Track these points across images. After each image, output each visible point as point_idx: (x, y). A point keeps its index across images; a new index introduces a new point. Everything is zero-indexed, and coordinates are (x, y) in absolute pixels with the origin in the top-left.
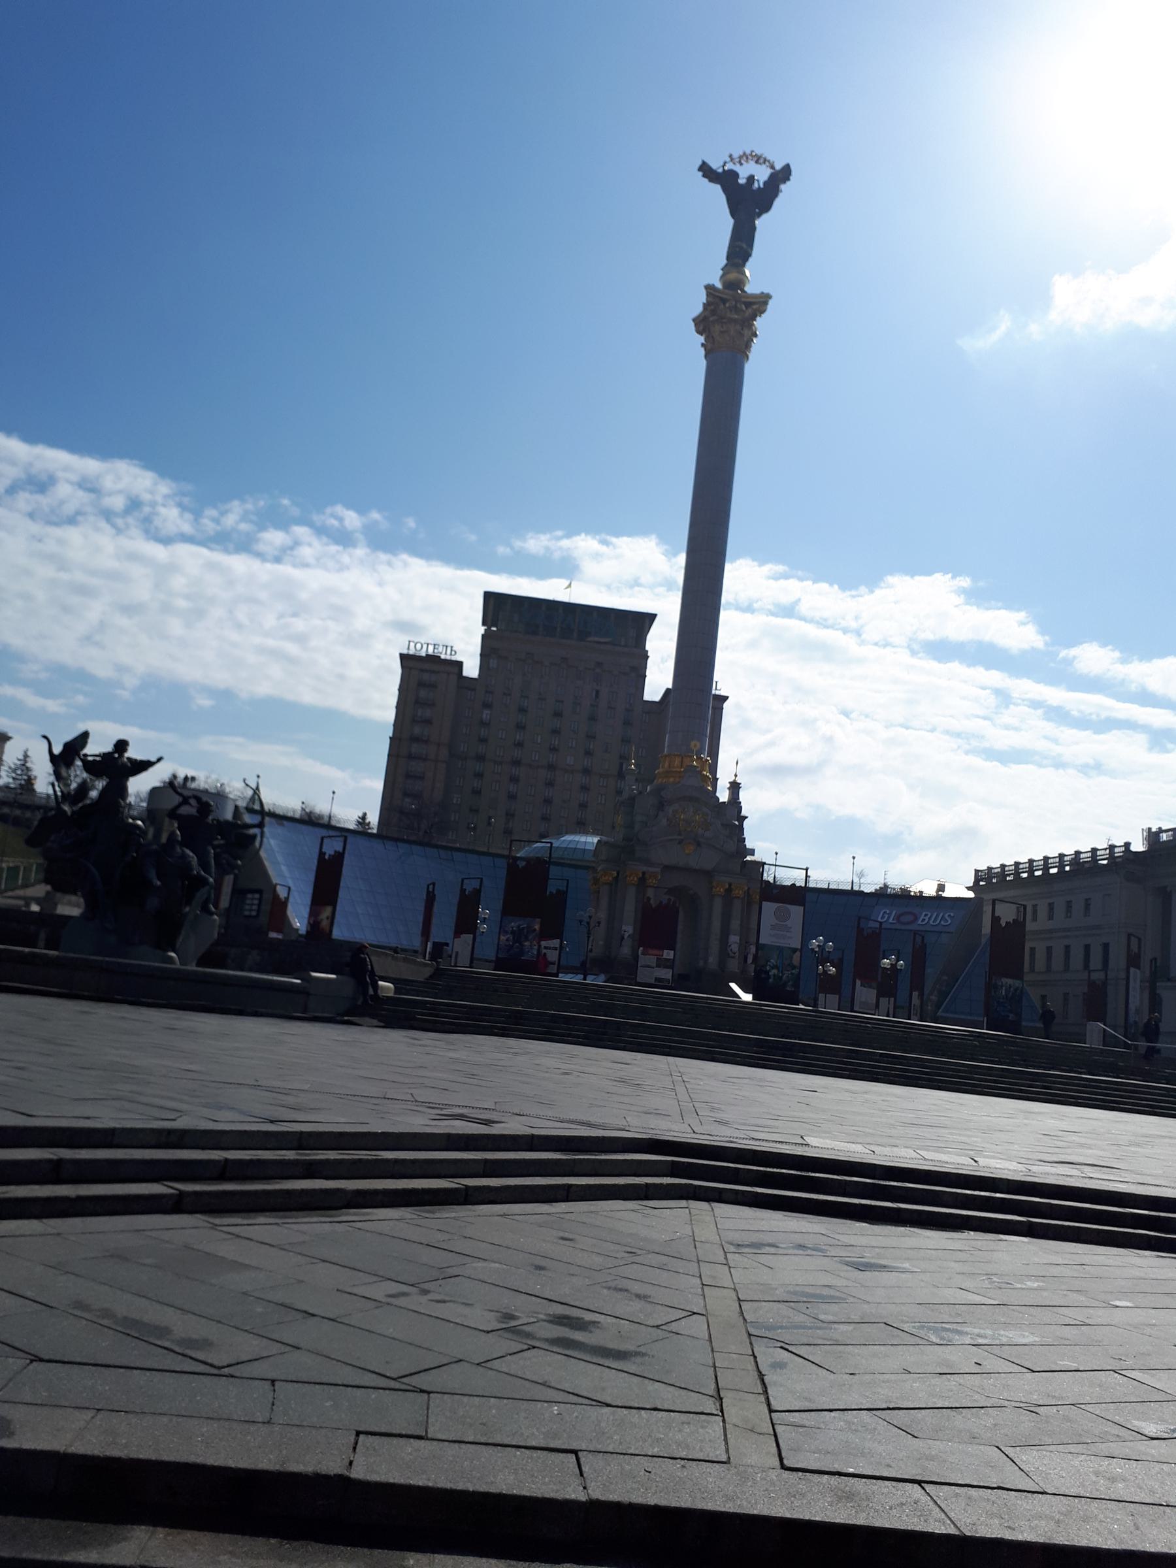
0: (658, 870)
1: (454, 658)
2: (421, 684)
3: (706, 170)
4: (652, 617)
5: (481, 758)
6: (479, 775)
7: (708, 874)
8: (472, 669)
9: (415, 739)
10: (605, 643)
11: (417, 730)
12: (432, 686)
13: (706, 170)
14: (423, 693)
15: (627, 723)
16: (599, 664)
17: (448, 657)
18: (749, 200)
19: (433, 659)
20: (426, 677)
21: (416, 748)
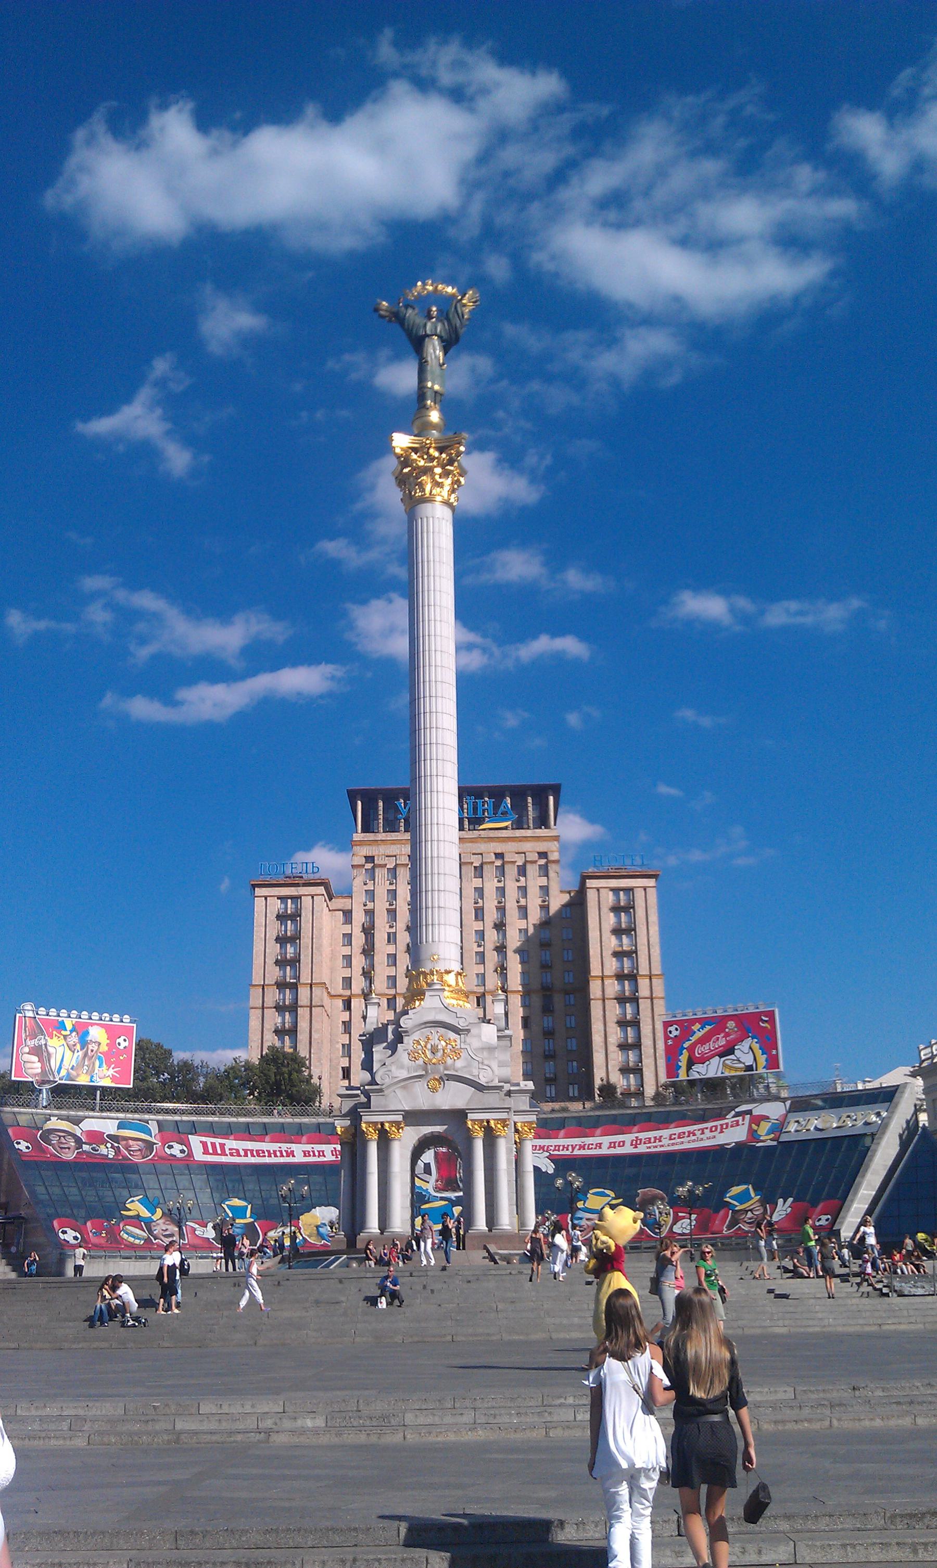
0: (400, 1118)
1: (317, 876)
7: (459, 1116)
9: (281, 985)
10: (506, 828)
15: (545, 924)
16: (500, 856)
17: (311, 876)
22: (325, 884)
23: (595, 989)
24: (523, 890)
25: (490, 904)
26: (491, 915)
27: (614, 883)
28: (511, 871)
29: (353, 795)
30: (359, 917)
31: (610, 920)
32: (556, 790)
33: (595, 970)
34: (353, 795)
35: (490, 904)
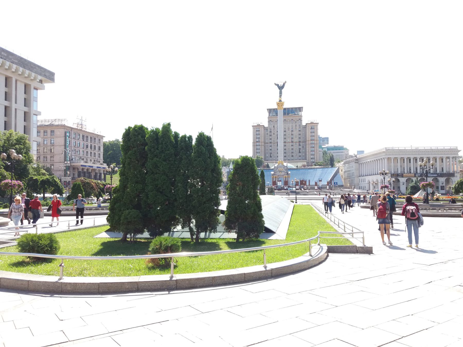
2: (257, 131)
3: (276, 84)
4: (302, 107)
5: (271, 143)
6: (271, 146)
8: (266, 125)
9: (257, 142)
11: (257, 140)
12: (259, 131)
13: (276, 84)
14: (257, 133)
16: (292, 120)
18: (281, 88)
19: (259, 125)
20: (257, 129)
21: (257, 144)
22: (264, 126)
23: (307, 143)
24: (296, 126)
25: (290, 128)
26: (290, 131)
27: (311, 125)
28: (294, 122)
29: (268, 109)
30: (269, 130)
31: (311, 130)
32: (302, 107)
33: (307, 139)
34: (268, 109)
35: (290, 128)
